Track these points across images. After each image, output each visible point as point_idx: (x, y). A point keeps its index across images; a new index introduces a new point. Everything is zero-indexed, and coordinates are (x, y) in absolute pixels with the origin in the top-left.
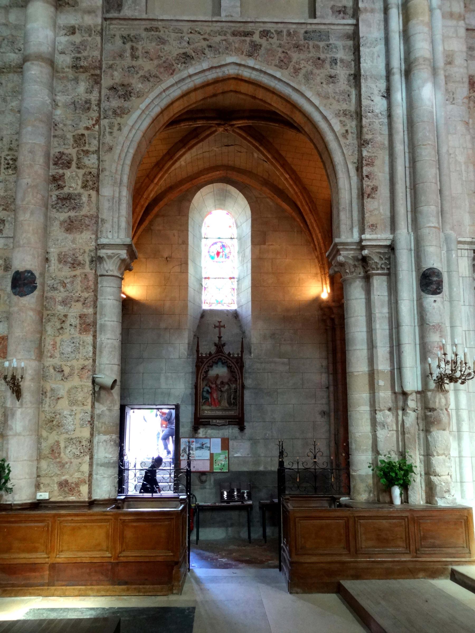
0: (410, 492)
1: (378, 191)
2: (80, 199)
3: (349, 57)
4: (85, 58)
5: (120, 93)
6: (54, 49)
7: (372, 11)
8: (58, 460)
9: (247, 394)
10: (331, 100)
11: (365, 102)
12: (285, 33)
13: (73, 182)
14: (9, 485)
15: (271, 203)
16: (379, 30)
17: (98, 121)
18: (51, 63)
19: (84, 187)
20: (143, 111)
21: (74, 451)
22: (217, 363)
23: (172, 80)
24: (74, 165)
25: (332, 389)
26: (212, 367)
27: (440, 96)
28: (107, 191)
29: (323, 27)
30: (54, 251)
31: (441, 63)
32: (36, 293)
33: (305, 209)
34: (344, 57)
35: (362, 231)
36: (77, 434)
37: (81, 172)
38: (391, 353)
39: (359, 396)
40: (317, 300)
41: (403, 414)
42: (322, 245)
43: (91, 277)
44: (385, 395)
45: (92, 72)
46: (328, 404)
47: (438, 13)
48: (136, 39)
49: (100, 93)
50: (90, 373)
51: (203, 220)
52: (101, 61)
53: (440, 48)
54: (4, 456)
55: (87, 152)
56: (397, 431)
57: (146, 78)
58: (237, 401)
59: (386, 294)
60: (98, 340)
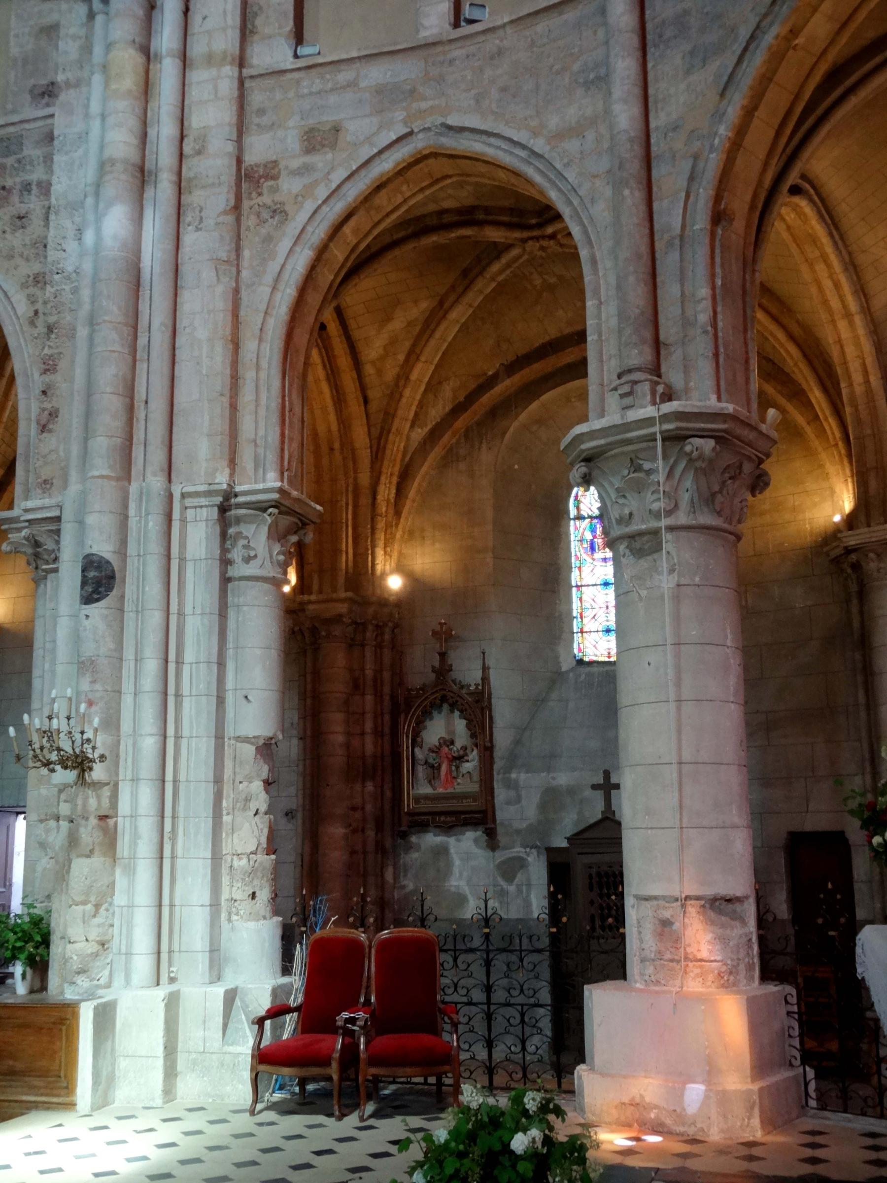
1: (59, 418)
29: (11, 129)
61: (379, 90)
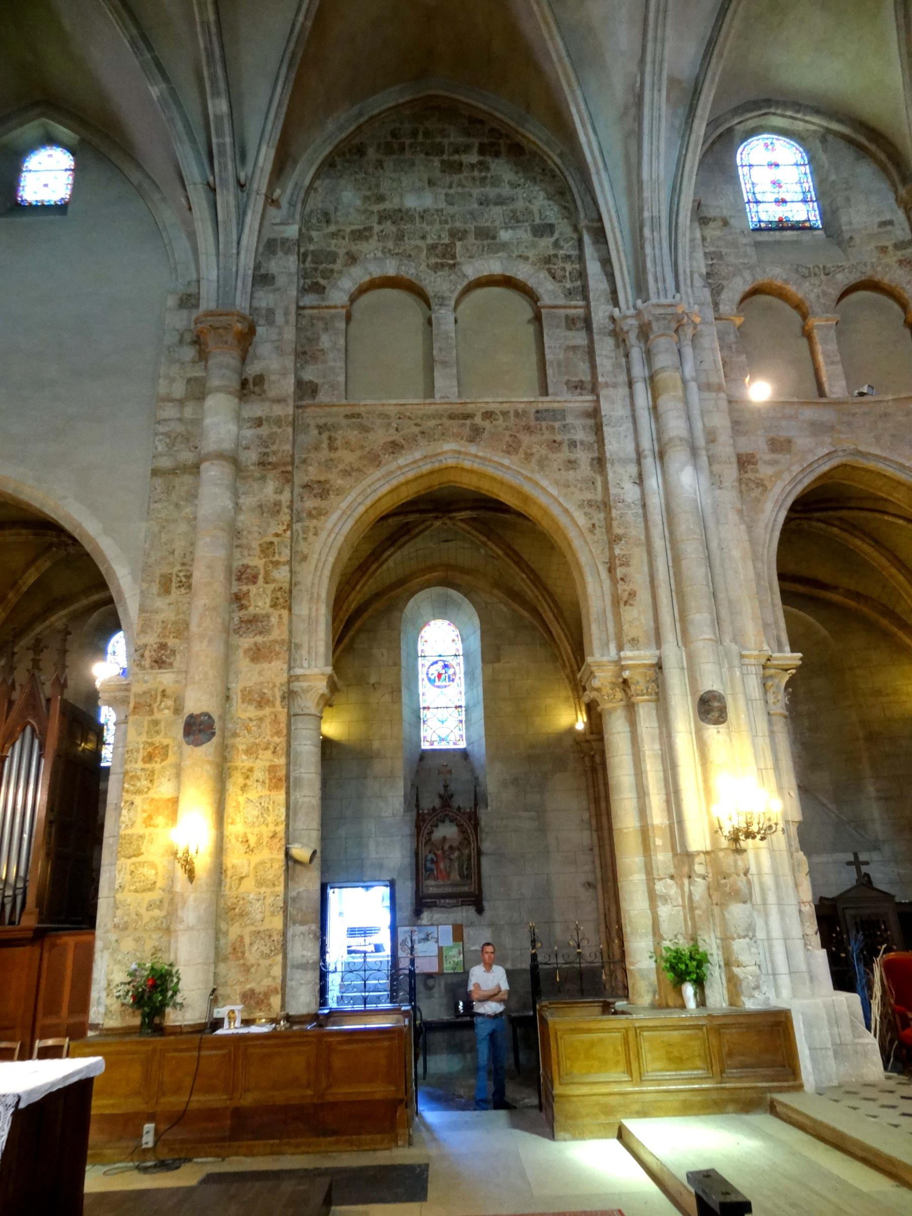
0: (708, 991)
2: (269, 621)
3: (591, 438)
4: (274, 453)
5: (315, 491)
6: (237, 446)
7: (615, 386)
8: (242, 962)
9: (485, 861)
10: (572, 489)
11: (613, 490)
12: (512, 413)
13: (260, 601)
14: (179, 999)
15: (505, 609)
16: (624, 406)
17: (290, 526)
18: (234, 461)
19: (274, 605)
20: (344, 512)
21: (262, 948)
22: (443, 821)
23: (378, 473)
24: (261, 579)
25: (596, 850)
26: (437, 826)
27: (704, 481)
28: (302, 609)
30: (237, 687)
31: (701, 442)
32: (215, 740)
33: (549, 616)
34: (585, 439)
35: (620, 648)
36: (266, 926)
37: (271, 586)
38: (668, 802)
39: (630, 860)
40: (571, 730)
41: (690, 884)
42: (573, 660)
43: (283, 718)
44: (663, 858)
45: (283, 469)
46: (594, 872)
47: (693, 386)
48: (334, 427)
49: (292, 492)
50: (283, 842)
51: (419, 633)
52: (293, 456)
53: (698, 426)
54: (172, 958)
55: (276, 564)
56: (683, 907)
57: (346, 473)
58: (472, 871)
59: (656, 725)
60: (292, 798)
61: (812, 424)
